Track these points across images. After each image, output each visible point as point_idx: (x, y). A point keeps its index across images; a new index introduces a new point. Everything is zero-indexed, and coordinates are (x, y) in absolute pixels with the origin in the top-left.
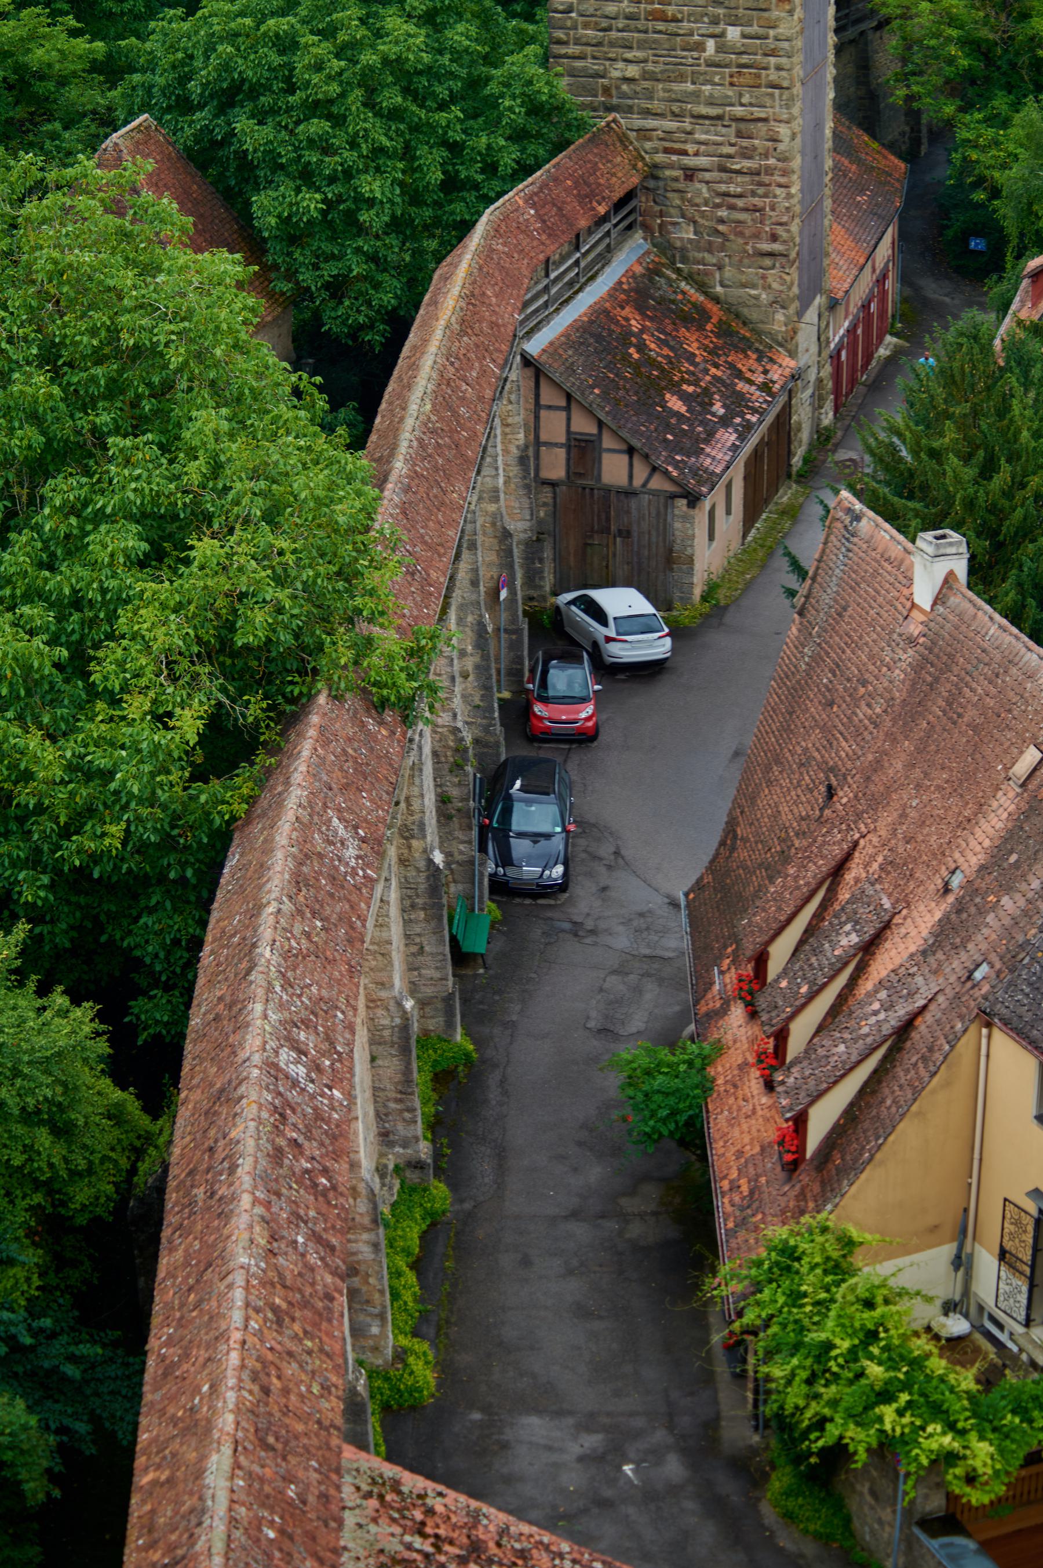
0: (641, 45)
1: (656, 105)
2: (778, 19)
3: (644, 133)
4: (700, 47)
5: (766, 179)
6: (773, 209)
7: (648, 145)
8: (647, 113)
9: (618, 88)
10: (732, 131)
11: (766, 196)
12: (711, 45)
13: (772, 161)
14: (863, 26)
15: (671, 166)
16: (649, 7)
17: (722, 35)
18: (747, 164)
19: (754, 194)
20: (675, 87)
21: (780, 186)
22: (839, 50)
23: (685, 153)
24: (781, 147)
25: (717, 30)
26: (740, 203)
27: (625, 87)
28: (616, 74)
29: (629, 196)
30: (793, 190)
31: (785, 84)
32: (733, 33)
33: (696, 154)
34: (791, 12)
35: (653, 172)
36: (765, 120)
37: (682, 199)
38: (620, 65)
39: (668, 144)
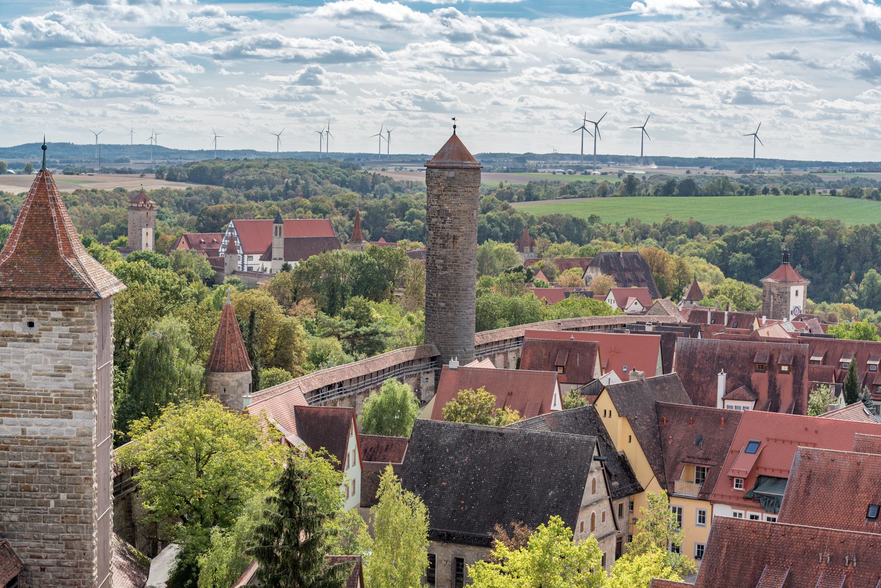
0: (19, 504)
1: (26, 534)
2: (85, 488)
3: (21, 549)
4: (47, 504)
5: (80, 569)
6: (84, 584)
7: (23, 554)
8: (22, 538)
9: (7, 526)
10: (64, 545)
11: (80, 577)
12: (52, 502)
13: (83, 560)
14: (128, 491)
15: (34, 564)
16: (22, 485)
17: (58, 497)
18: (70, 563)
19: (74, 576)
20: (36, 525)
21: (87, 572)
22: (116, 503)
23: (40, 558)
24: (87, 552)
25: (56, 496)
26: (68, 582)
27: (11, 525)
28: (6, 519)
29: (14, 580)
30: (94, 574)
31: (89, 521)
32: (63, 496)
33: (46, 558)
34: (91, 485)
35: (25, 568)
36: (80, 540)
37: (40, 581)
38: (9, 514)
39: (32, 554)
